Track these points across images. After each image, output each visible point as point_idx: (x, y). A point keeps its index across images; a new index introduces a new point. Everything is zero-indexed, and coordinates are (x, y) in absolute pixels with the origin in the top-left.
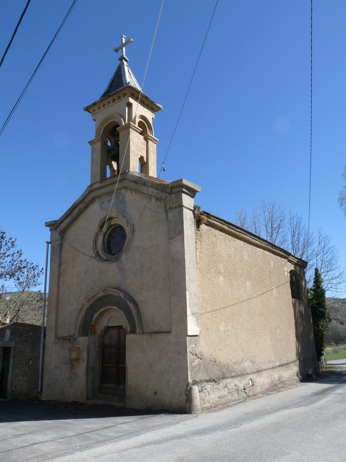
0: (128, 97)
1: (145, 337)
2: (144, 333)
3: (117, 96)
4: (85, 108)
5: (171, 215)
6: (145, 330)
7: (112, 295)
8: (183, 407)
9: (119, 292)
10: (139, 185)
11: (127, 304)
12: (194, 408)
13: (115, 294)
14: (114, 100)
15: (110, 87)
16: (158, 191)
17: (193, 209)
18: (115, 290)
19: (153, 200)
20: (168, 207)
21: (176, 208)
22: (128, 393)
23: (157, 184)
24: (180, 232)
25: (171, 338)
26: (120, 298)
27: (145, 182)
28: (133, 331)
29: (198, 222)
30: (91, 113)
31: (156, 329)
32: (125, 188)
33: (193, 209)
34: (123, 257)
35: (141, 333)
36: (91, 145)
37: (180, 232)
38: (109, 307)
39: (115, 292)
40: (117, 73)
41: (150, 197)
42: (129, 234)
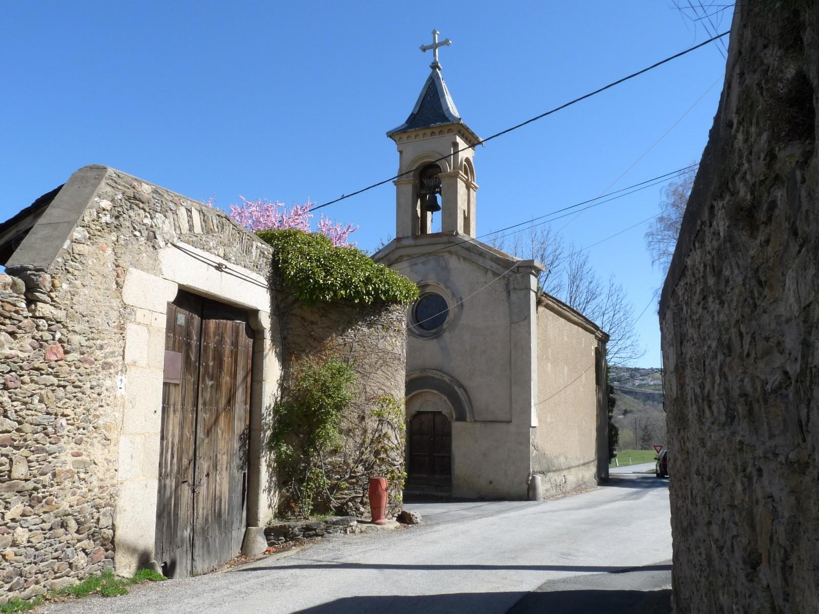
0: (455, 134)
1: (478, 425)
2: (475, 421)
3: (439, 130)
4: (389, 134)
5: (514, 296)
6: (477, 419)
7: (433, 378)
8: (528, 494)
9: (443, 375)
10: (472, 254)
11: (451, 389)
12: (539, 496)
13: (436, 376)
14: (433, 133)
15: (421, 104)
16: (498, 266)
17: (536, 291)
18: (438, 372)
19: (490, 274)
20: (511, 287)
21: (522, 289)
22: (455, 482)
23: (498, 258)
24: (526, 317)
25: (512, 428)
26: (444, 382)
27: (482, 253)
28: (461, 418)
29: (539, 303)
30: (395, 141)
31: (490, 418)
32: (450, 252)
33: (536, 291)
34: (447, 336)
35: (473, 421)
36: (395, 185)
37: (526, 317)
38: (425, 390)
39: (436, 374)
40: (429, 88)
41: (486, 270)
42: (452, 305)
